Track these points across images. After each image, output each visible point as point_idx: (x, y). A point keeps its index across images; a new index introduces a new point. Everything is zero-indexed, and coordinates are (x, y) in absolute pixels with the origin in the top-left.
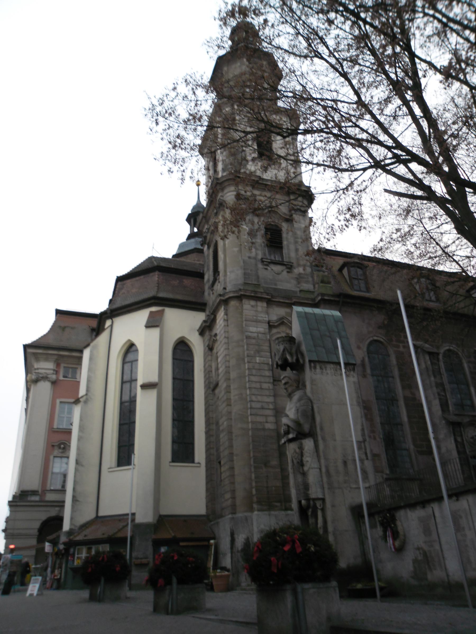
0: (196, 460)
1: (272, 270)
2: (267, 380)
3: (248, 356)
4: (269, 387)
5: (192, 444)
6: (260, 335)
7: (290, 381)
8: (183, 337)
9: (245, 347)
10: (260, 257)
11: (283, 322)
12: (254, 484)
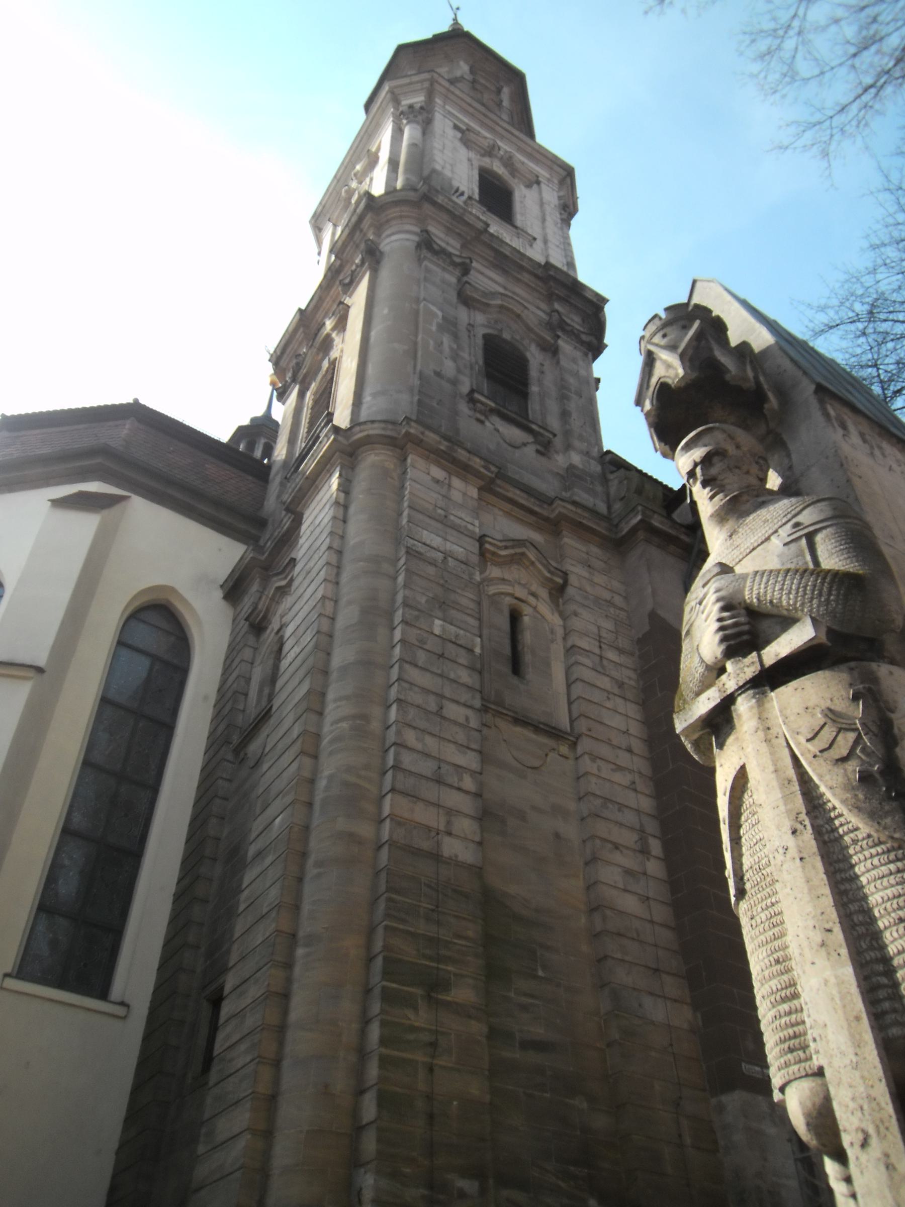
0: (117, 990)
1: (497, 430)
2: (465, 697)
3: (406, 604)
4: (467, 719)
5: (117, 932)
7: (731, 449)
8: (172, 590)
9: (401, 579)
10: (465, 389)
11: (523, 554)
12: (373, 1071)
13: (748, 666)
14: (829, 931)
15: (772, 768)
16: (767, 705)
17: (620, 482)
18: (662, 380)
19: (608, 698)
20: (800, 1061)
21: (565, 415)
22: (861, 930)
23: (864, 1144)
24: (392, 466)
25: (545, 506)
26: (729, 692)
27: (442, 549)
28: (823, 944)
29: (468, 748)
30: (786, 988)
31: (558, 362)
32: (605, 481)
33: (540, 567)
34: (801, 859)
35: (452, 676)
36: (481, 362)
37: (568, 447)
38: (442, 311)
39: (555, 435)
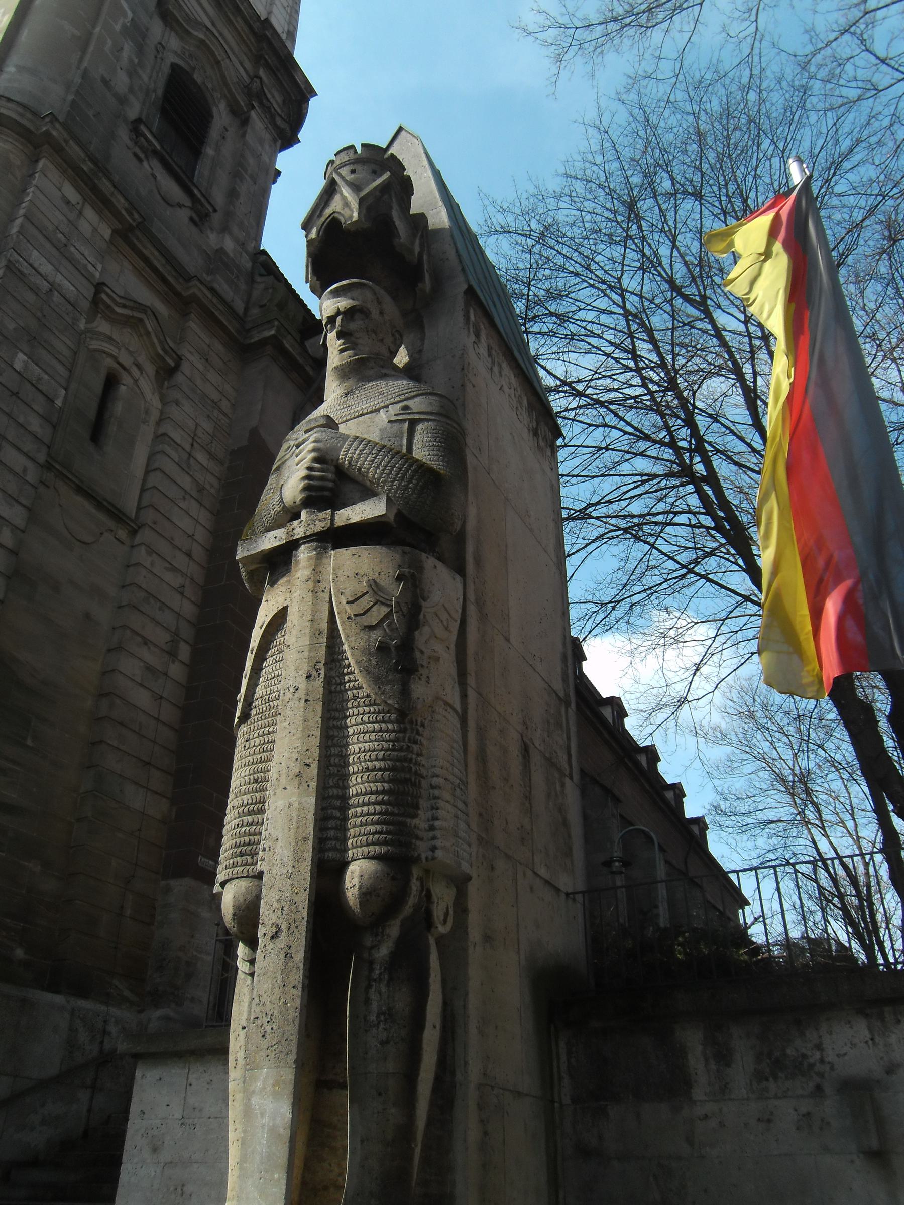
1: (155, 177)
4: (25, 470)
6: (56, 297)
7: (375, 314)
10: (133, 112)
13: (320, 520)
14: (308, 765)
15: (309, 617)
16: (325, 561)
17: (266, 289)
18: (336, 215)
19: (184, 498)
20: (246, 864)
21: (233, 194)
22: (333, 770)
24: (18, 162)
25: (181, 280)
26: (296, 537)
27: (51, 279)
29: (17, 501)
30: (256, 804)
31: (244, 135)
32: (251, 281)
33: (155, 341)
34: (306, 701)
35: (21, 420)
36: (160, 92)
37: (225, 229)
38: (133, 12)
39: (215, 211)
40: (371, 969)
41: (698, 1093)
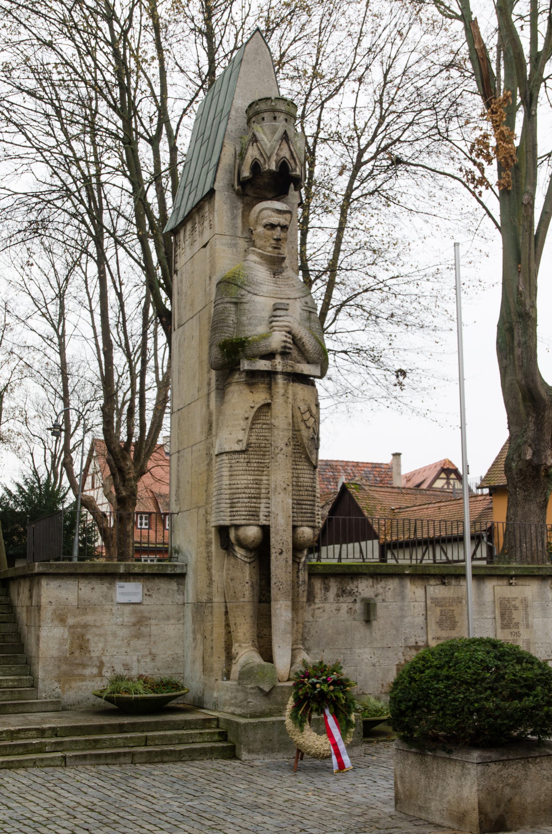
23: (281, 553)
28: (285, 489)
40: (299, 566)
41: (317, 601)
